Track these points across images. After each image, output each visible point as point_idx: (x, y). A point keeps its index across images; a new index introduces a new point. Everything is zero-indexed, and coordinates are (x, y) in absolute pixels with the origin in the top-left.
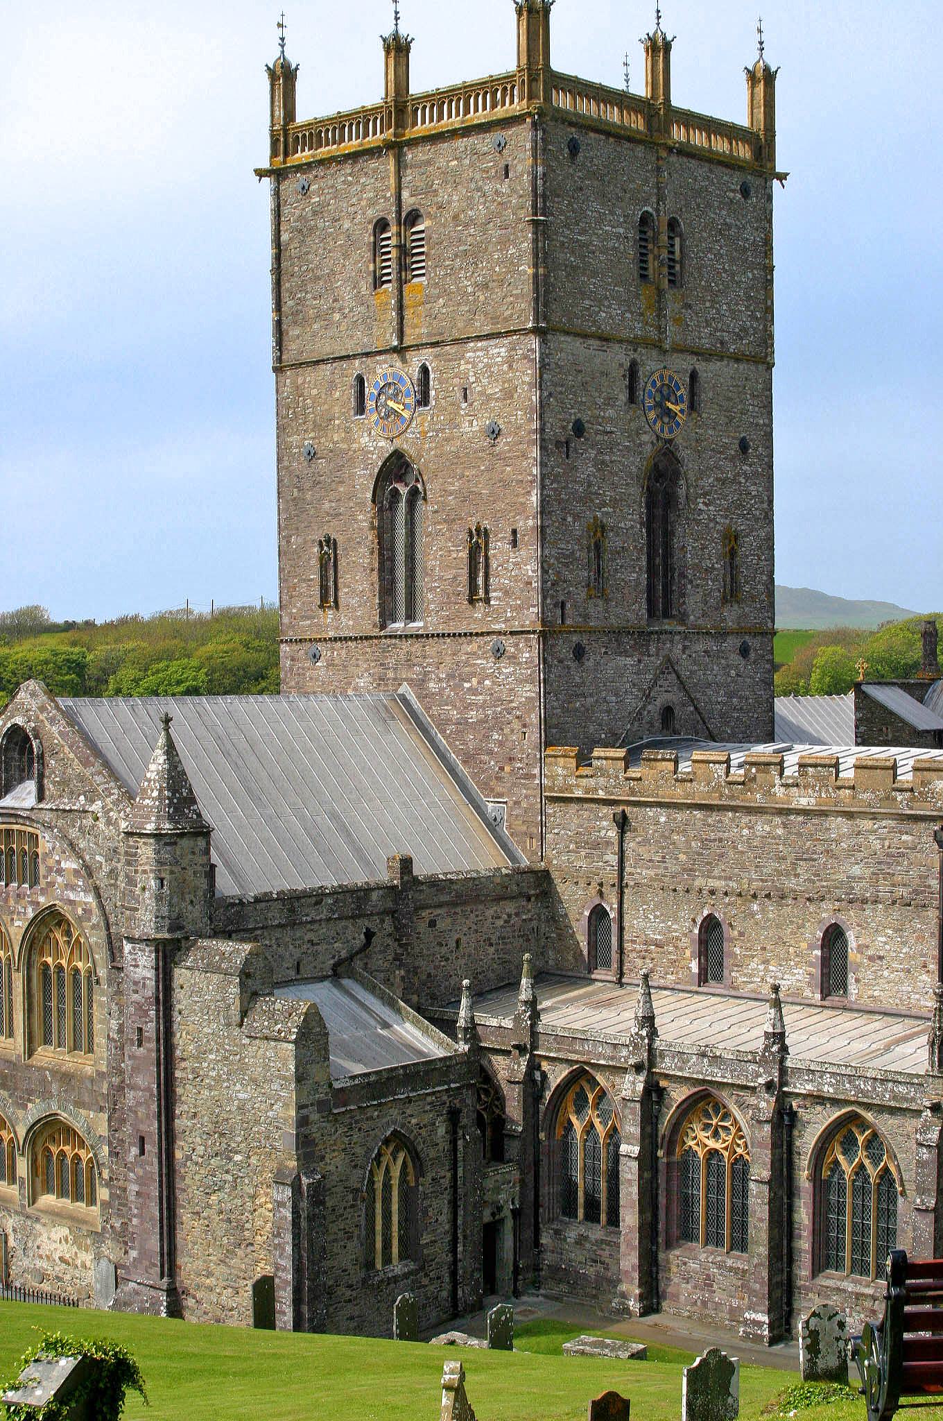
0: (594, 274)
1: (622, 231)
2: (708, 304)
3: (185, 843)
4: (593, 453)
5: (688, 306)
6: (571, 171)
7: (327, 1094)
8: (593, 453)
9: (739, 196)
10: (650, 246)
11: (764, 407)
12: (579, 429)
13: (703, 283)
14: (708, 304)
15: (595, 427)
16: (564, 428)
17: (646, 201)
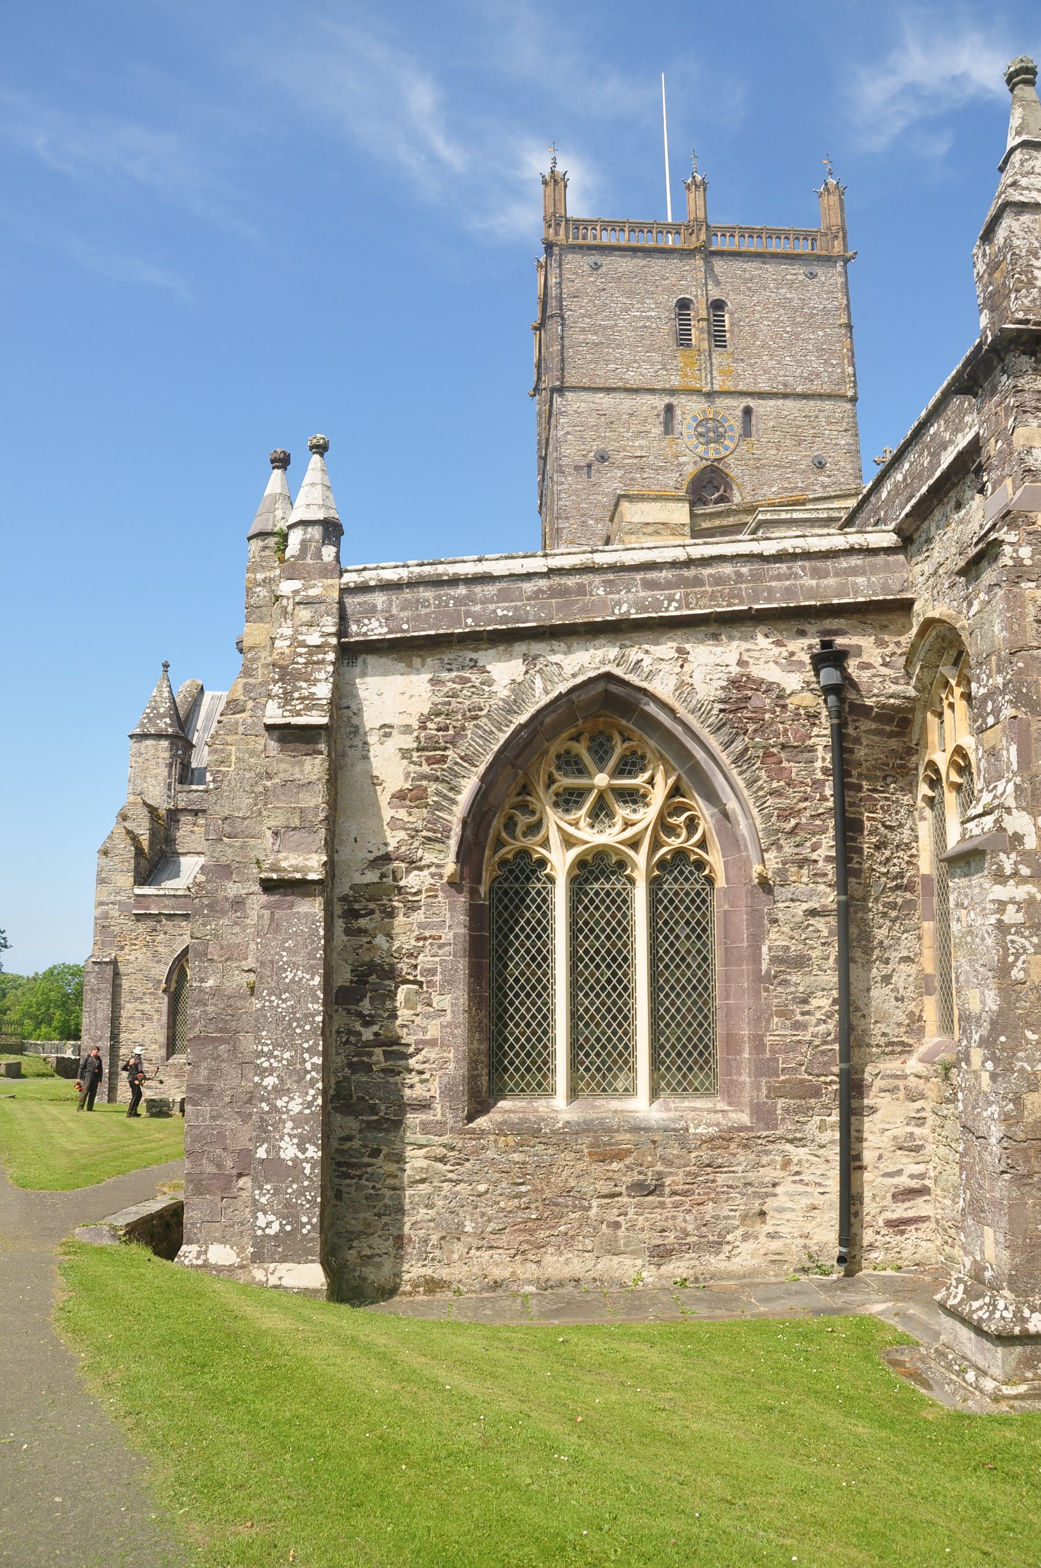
0: (619, 346)
1: (653, 314)
2: (764, 358)
3: (150, 742)
4: (620, 473)
5: (736, 361)
6: (592, 279)
7: (129, 898)
8: (620, 473)
9: (801, 277)
10: (692, 323)
11: (846, 431)
12: (603, 458)
13: (758, 343)
14: (764, 358)
15: (622, 454)
16: (584, 456)
17: (682, 291)
